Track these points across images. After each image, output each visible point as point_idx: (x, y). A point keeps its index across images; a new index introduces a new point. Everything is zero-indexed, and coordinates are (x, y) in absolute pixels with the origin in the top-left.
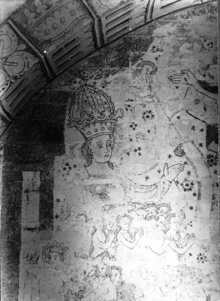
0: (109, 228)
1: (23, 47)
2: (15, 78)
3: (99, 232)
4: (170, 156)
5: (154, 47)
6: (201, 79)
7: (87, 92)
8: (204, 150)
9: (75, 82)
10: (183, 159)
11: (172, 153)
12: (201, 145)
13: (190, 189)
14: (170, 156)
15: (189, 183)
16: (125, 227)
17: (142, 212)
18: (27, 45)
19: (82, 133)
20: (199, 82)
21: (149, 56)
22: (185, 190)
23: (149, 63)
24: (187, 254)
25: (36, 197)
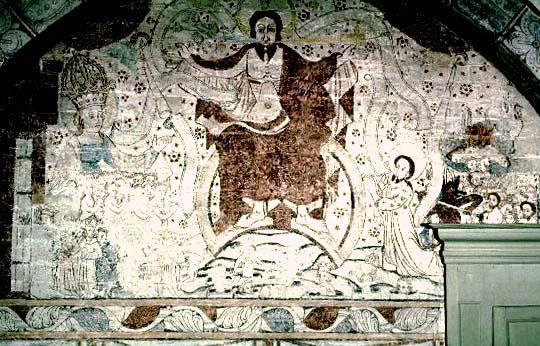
0: (97, 193)
1: (17, 26)
2: (9, 55)
3: (88, 197)
4: (159, 128)
5: (149, 18)
6: (195, 52)
7: (81, 62)
8: (192, 123)
9: (69, 52)
10: (172, 132)
11: (162, 126)
12: (190, 118)
13: (177, 161)
14: (159, 128)
15: (176, 155)
16: (112, 194)
17: (131, 181)
18: (21, 24)
19: (75, 104)
20: (193, 55)
21: (144, 26)
22: (172, 161)
23: (143, 34)
24: (170, 220)
25: (28, 164)
